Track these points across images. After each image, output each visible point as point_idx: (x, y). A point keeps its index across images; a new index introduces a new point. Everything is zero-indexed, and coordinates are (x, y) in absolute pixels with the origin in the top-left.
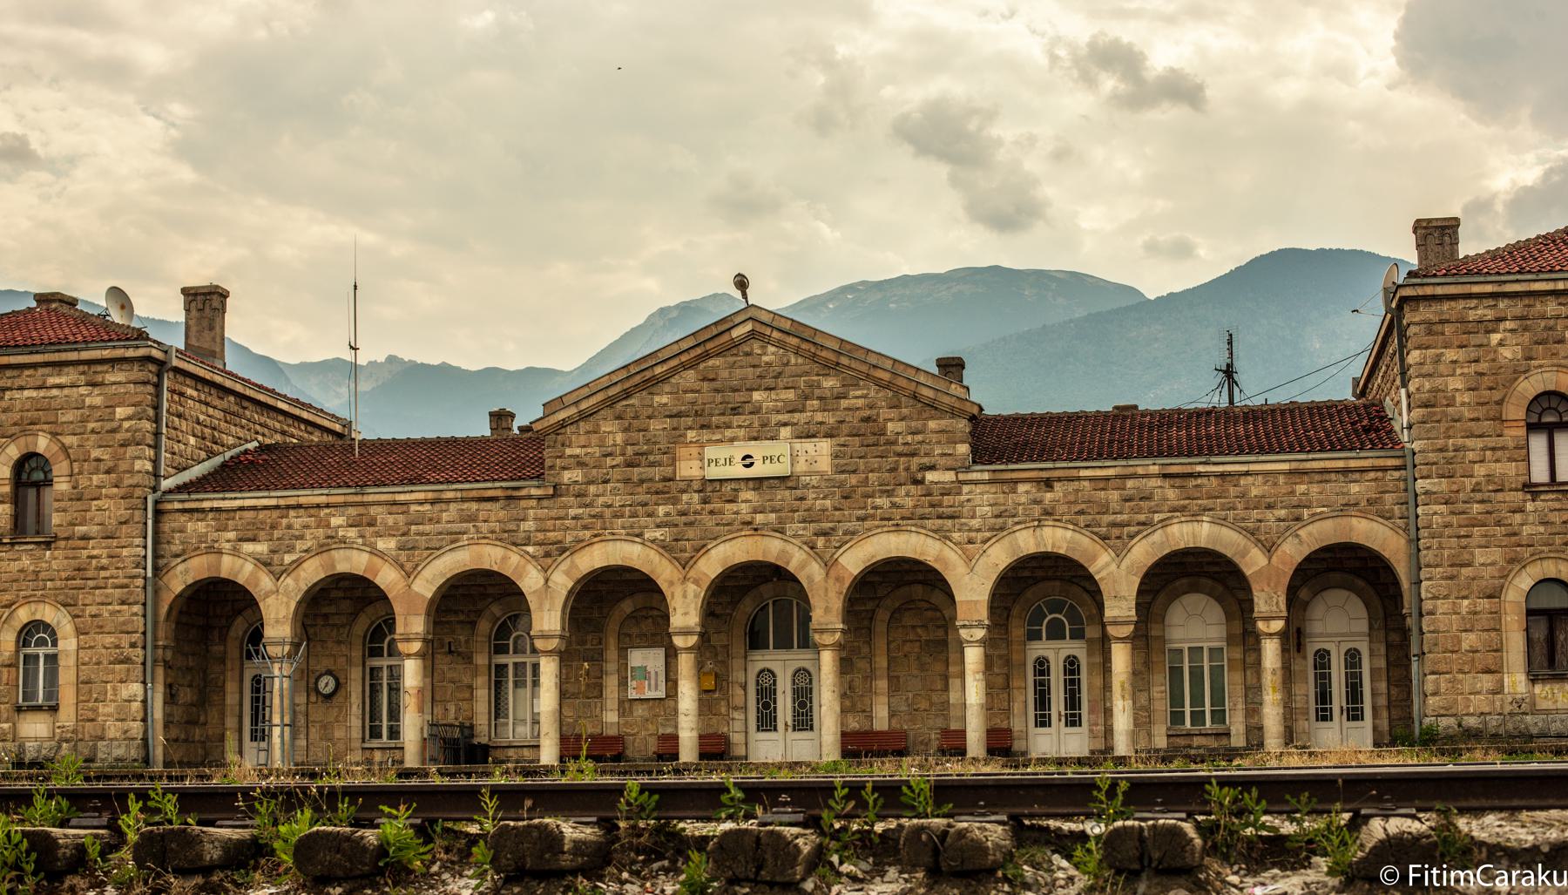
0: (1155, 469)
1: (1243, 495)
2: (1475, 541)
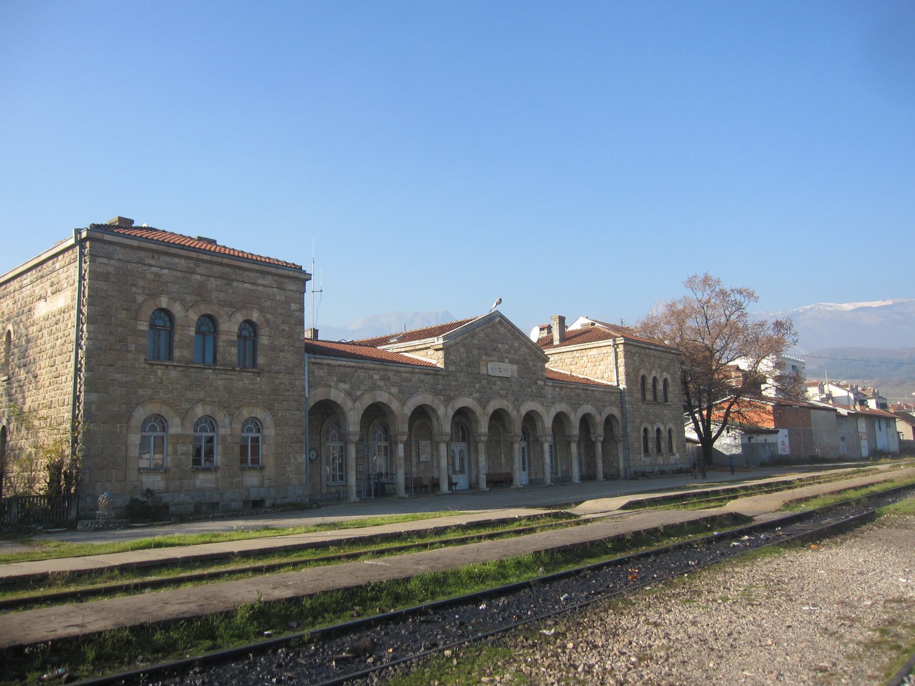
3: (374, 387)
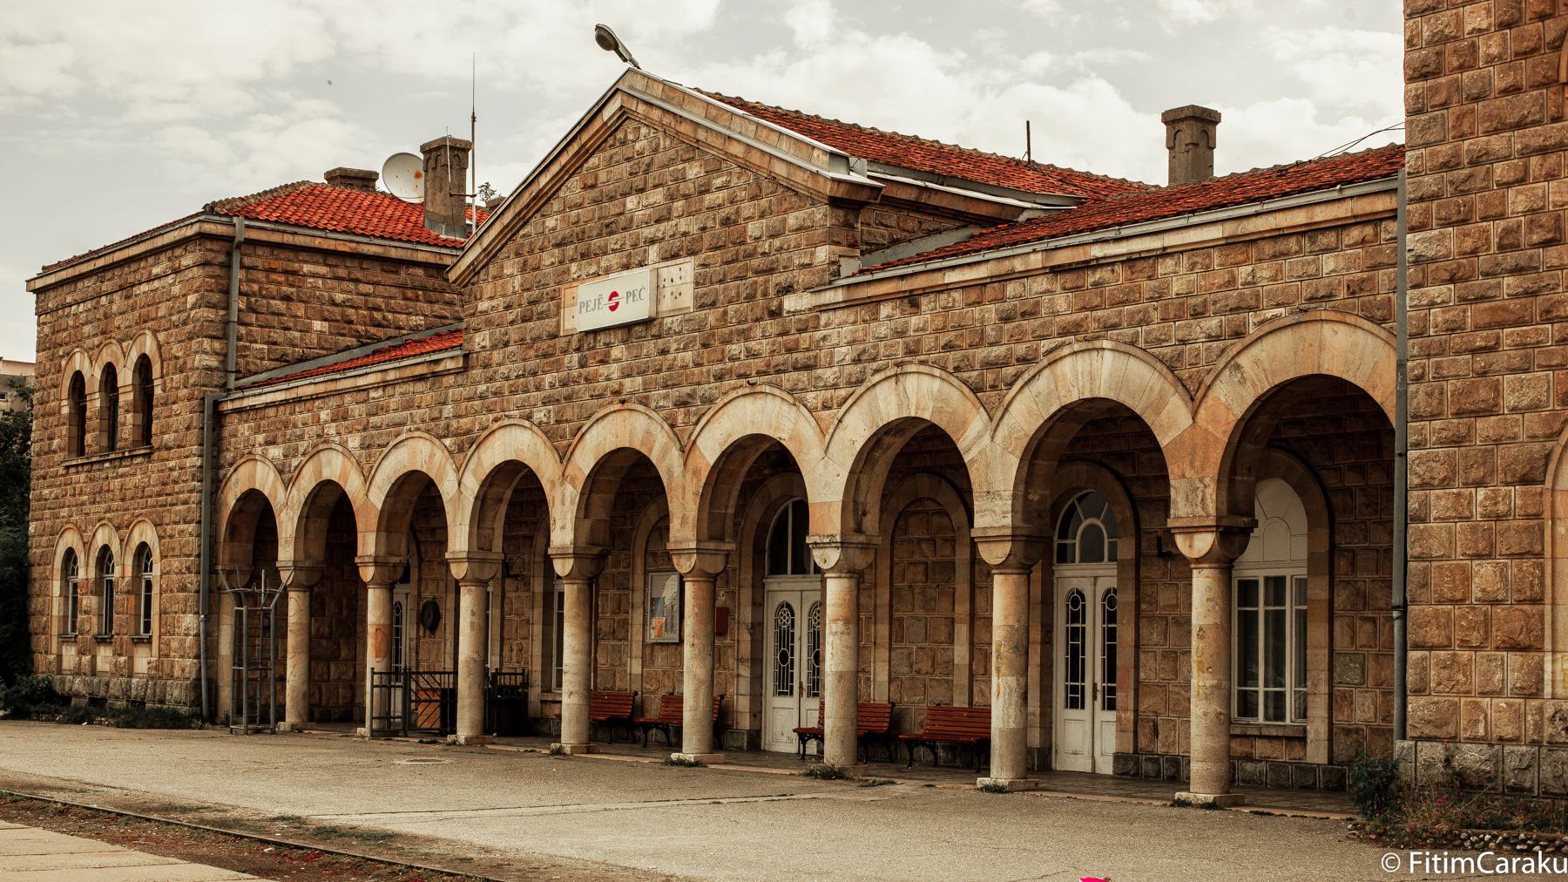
0: (1036, 261)
1: (1158, 296)
2: (1508, 354)
3: (322, 443)
